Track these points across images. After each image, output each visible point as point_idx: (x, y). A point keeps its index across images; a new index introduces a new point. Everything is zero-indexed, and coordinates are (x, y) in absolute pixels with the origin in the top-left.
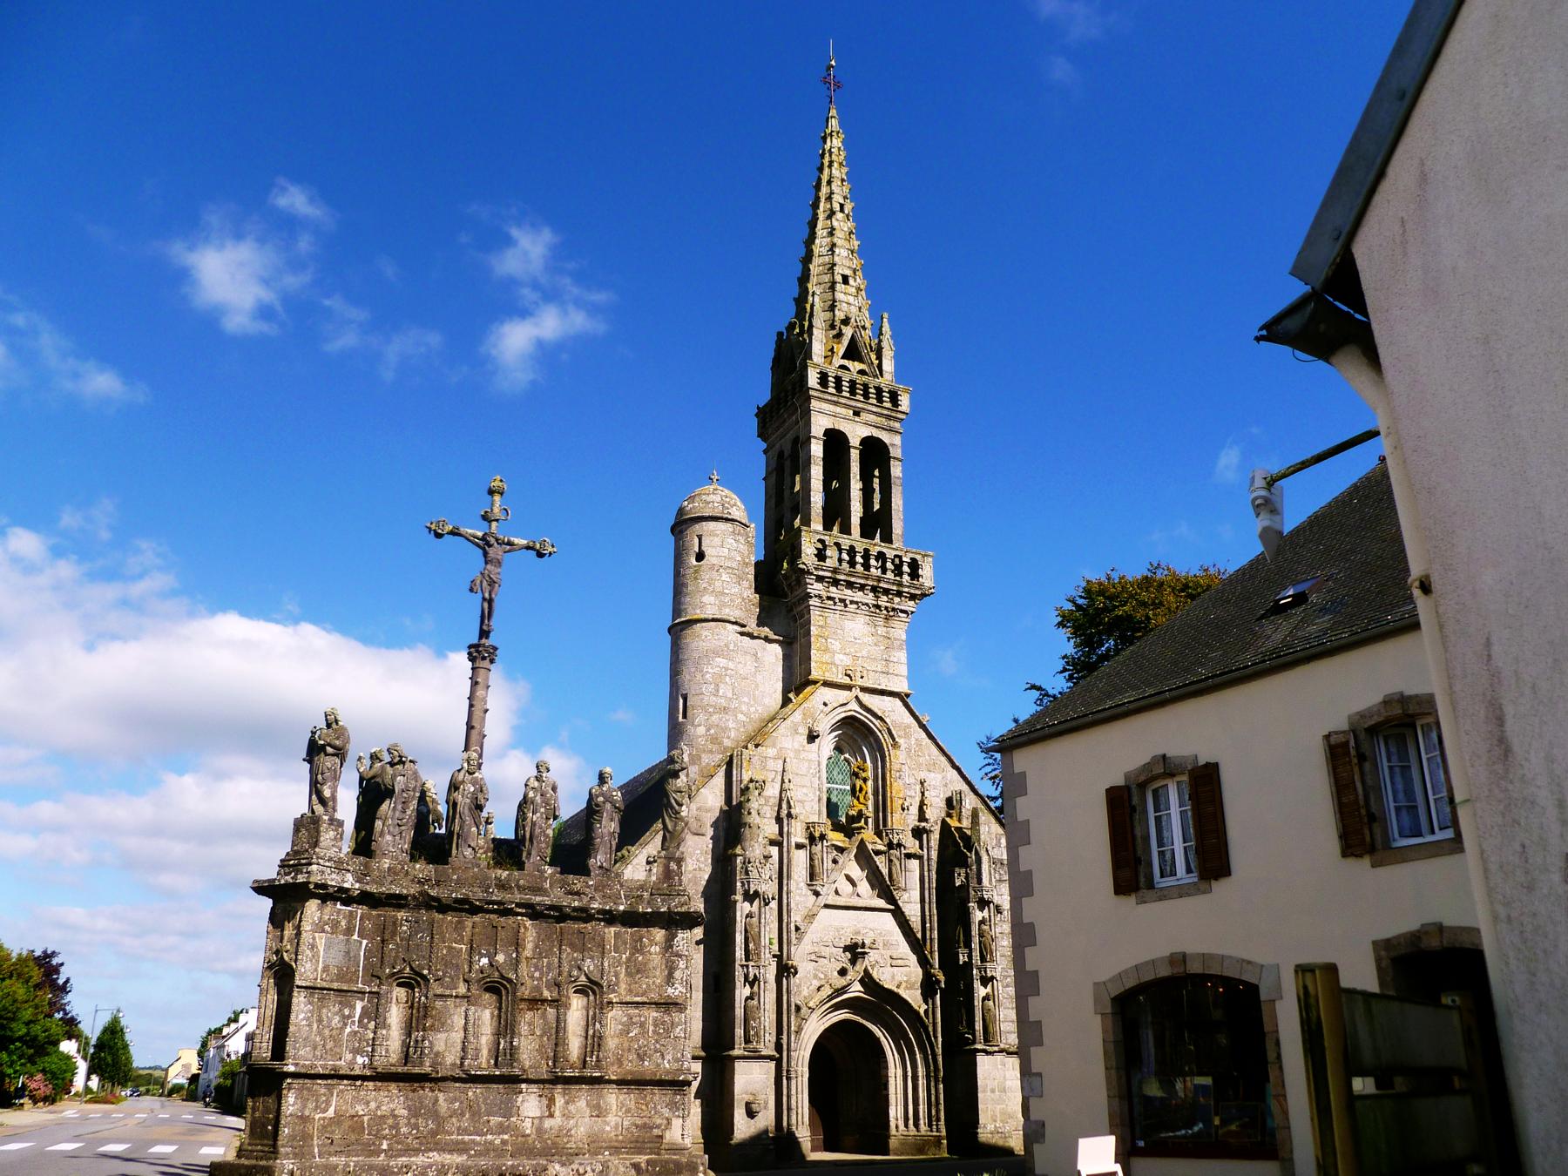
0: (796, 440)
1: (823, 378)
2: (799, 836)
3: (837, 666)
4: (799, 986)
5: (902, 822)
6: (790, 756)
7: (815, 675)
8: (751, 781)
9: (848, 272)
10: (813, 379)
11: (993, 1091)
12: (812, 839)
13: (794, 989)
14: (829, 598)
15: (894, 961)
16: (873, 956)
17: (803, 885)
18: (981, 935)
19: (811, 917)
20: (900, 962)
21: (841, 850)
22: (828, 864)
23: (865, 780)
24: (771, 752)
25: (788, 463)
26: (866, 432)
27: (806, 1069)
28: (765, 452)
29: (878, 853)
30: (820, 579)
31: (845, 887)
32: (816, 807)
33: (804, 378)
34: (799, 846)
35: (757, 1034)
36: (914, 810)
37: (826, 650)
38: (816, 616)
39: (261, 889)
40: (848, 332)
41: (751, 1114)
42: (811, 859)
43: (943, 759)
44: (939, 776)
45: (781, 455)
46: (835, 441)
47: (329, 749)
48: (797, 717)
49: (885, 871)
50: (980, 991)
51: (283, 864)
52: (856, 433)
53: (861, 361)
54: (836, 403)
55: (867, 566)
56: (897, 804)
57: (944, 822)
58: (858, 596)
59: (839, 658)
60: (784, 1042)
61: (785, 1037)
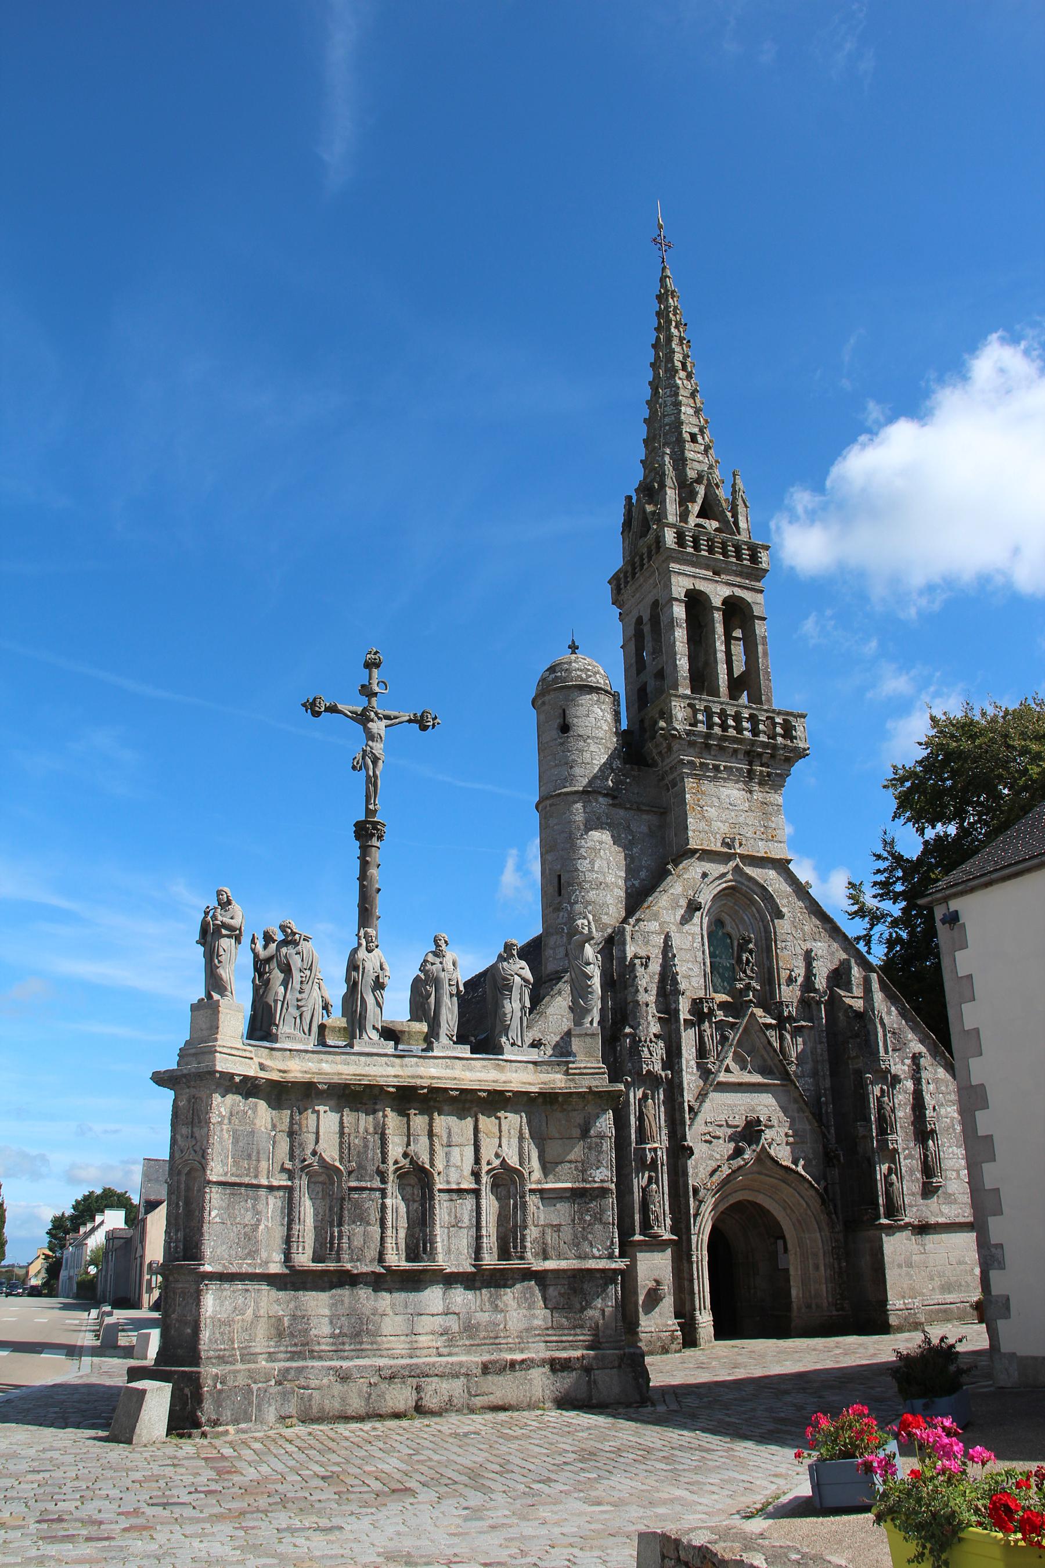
0: (656, 604)
3: (714, 834)
4: (695, 1167)
5: (789, 995)
6: (673, 929)
7: (693, 845)
8: (636, 957)
9: (696, 430)
10: (670, 537)
13: (690, 1171)
18: (880, 1107)
19: (702, 1096)
21: (732, 1026)
24: (654, 926)
25: (647, 629)
26: (727, 592)
27: (705, 1252)
29: (768, 1026)
33: (659, 540)
34: (688, 1023)
35: (657, 1218)
38: (690, 783)
39: (161, 1079)
40: (701, 490)
45: (639, 621)
46: (695, 601)
47: (224, 932)
49: (776, 1045)
51: (183, 1054)
52: (718, 593)
55: (739, 729)
56: (784, 974)
59: (717, 825)
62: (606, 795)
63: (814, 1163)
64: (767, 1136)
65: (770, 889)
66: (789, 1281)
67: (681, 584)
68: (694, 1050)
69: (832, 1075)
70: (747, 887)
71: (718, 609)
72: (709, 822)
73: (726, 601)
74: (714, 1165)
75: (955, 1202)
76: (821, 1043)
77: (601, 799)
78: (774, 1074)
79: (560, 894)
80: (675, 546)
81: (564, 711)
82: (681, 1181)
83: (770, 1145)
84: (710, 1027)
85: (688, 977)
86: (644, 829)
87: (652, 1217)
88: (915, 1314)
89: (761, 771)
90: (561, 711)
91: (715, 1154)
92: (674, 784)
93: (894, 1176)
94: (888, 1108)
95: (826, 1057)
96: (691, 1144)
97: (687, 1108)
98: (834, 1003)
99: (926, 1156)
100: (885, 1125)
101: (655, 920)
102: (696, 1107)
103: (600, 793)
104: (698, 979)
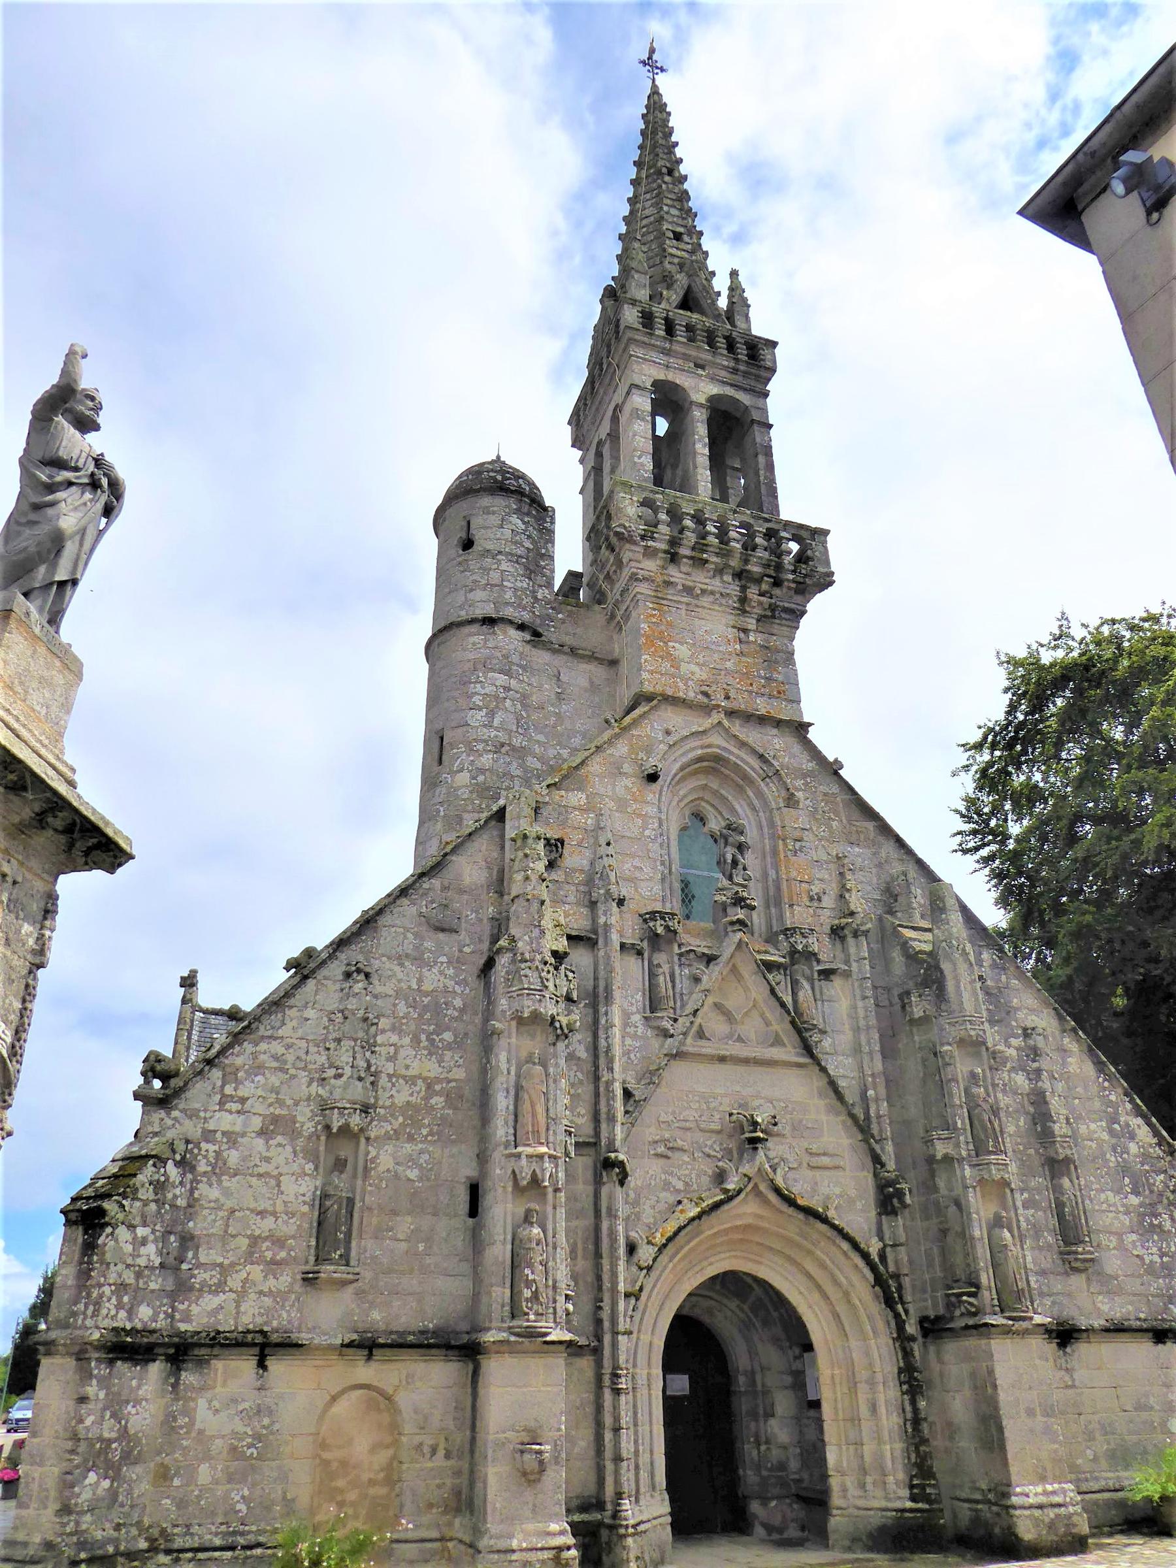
1: (647, 319)
2: (622, 926)
4: (636, 1203)
7: (648, 688)
11: (1030, 1413)
12: (654, 939)
14: (668, 584)
15: (815, 1161)
16: (775, 1148)
17: (637, 1018)
19: (652, 1076)
20: (825, 1160)
22: (683, 984)
23: (741, 847)
24: (576, 798)
26: (715, 390)
28: (582, 461)
30: (649, 553)
31: (715, 1025)
32: (657, 888)
35: (536, 1295)
36: (828, 902)
37: (668, 656)
41: (531, 1478)
42: (652, 975)
43: (870, 825)
44: (868, 852)
48: (621, 749)
50: (981, 1209)
52: (701, 389)
53: (703, 313)
54: (667, 352)
57: (880, 919)
58: (716, 584)
60: (605, 1315)
61: (606, 1305)
62: (522, 627)
63: (859, 1205)
64: (771, 1154)
65: (776, 763)
66: (821, 1430)
67: (648, 373)
68: (639, 996)
69: (884, 1057)
70: (738, 757)
71: (701, 405)
72: (676, 663)
73: (712, 399)
74: (672, 1199)
75: (1119, 1292)
76: (864, 998)
77: (513, 632)
78: (784, 1045)
79: (440, 762)
80: (640, 327)
81: (469, 523)
82: (605, 1225)
83: (774, 1171)
84: (670, 962)
85: (632, 880)
86: (583, 682)
87: (527, 1293)
88: (1070, 1516)
89: (760, 603)
90: (464, 523)
91: (674, 1181)
92: (627, 616)
93: (1006, 1234)
94: (985, 1106)
95: (873, 1022)
96: (621, 1157)
97: (619, 1093)
98: (887, 936)
99: (1060, 1205)
100: (984, 1142)
101: (579, 789)
102: (638, 1095)
103: (511, 622)
104: (651, 884)
